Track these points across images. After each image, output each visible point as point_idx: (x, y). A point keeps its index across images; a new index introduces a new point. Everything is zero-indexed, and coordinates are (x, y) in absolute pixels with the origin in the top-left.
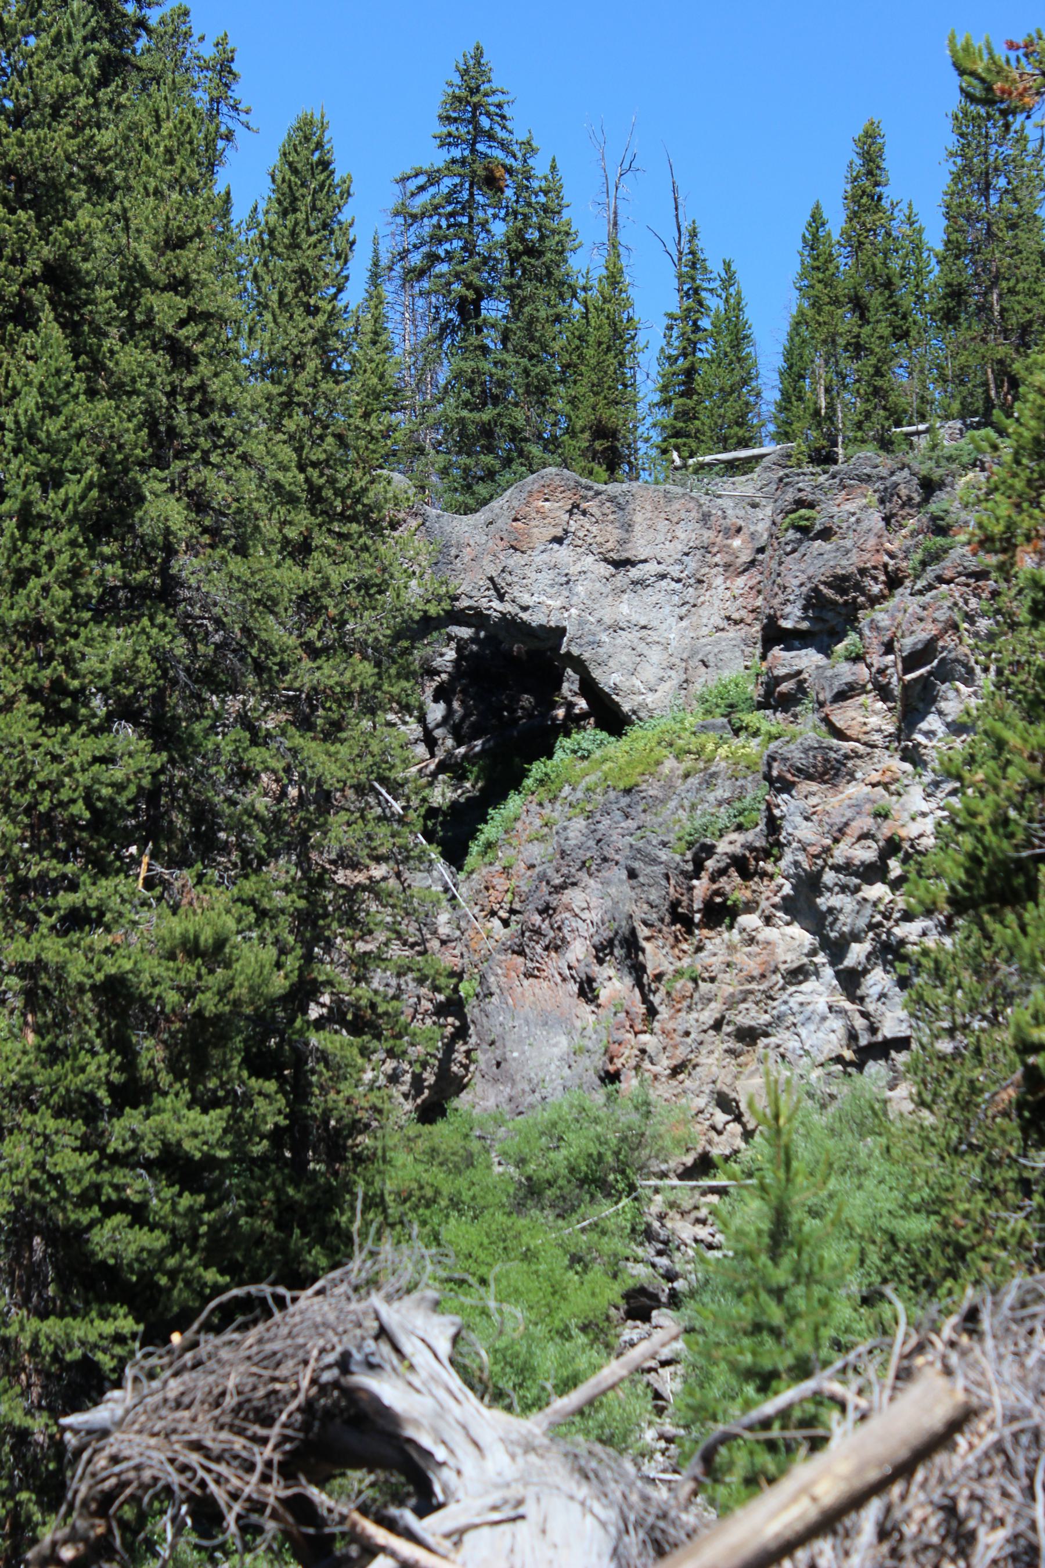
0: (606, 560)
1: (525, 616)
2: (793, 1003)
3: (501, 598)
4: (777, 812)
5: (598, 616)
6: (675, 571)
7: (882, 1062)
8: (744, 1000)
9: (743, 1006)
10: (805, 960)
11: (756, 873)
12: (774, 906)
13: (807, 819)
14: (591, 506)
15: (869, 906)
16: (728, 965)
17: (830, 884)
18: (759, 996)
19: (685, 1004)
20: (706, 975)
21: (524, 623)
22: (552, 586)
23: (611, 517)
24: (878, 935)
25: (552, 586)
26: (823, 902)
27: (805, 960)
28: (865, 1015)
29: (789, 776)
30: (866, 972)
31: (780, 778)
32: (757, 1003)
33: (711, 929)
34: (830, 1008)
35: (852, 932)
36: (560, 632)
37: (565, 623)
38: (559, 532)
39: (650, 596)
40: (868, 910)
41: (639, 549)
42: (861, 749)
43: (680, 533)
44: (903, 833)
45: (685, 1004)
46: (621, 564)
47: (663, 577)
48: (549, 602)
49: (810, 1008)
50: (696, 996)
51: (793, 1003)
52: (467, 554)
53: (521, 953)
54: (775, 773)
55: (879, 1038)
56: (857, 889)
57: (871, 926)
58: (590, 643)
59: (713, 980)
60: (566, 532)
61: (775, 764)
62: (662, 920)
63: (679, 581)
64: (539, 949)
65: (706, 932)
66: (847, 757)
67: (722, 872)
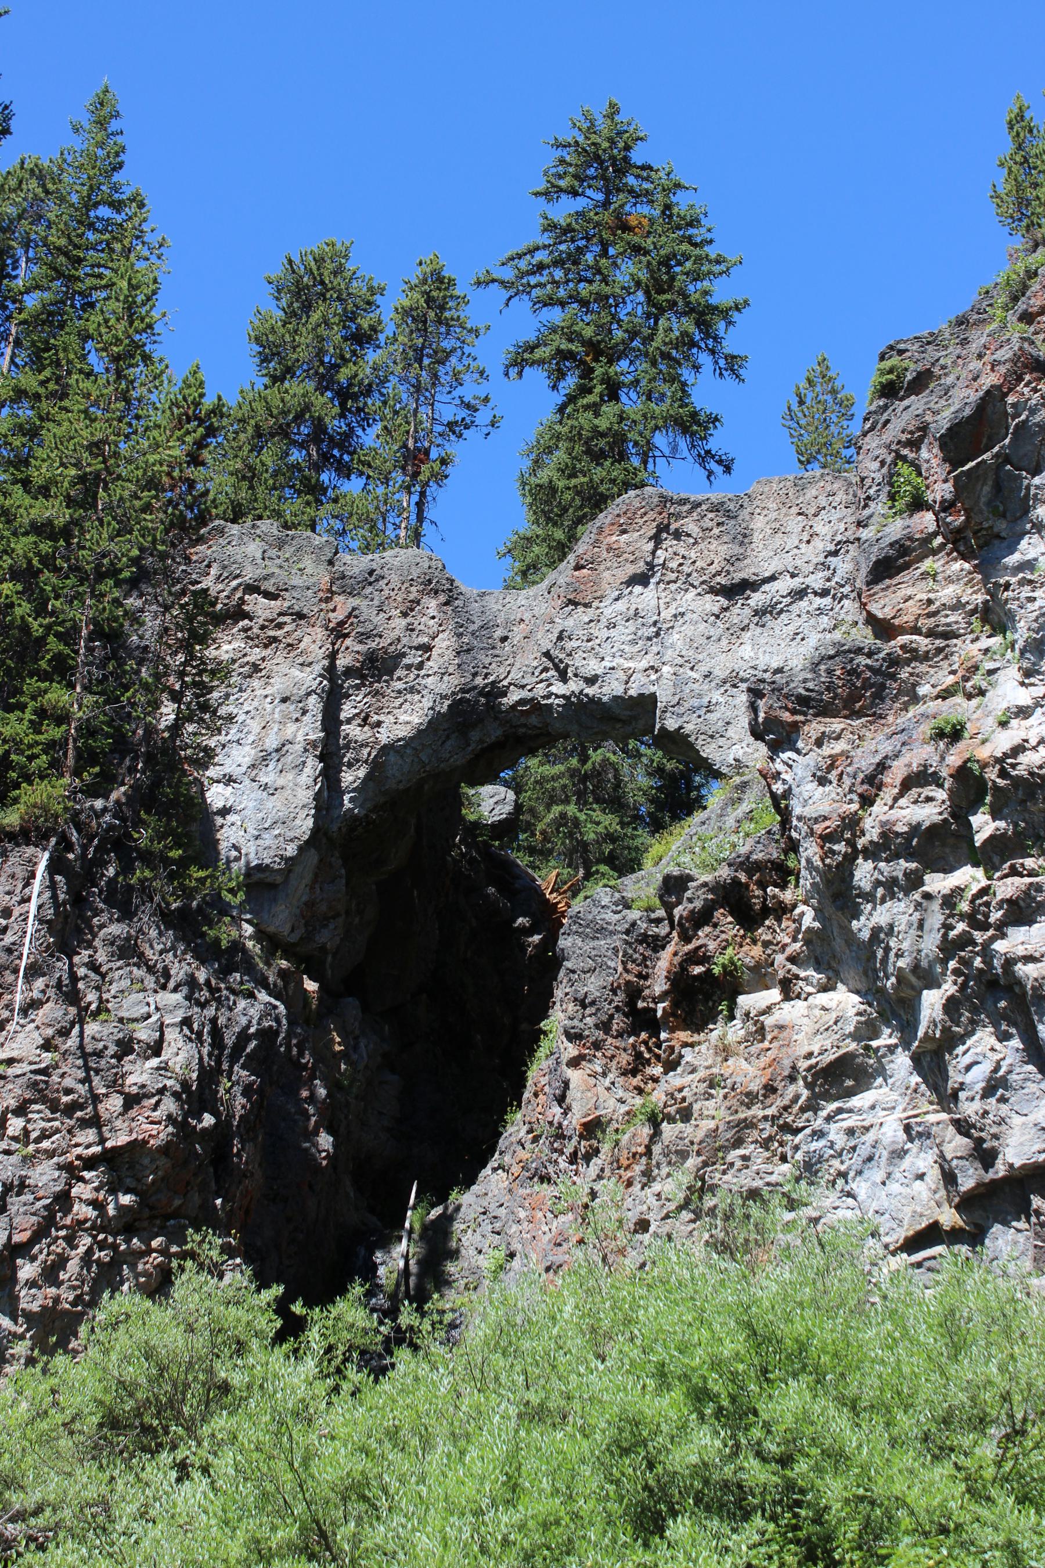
0: (713, 591)
1: (590, 691)
2: (835, 1133)
3: (563, 678)
4: (778, 788)
5: (703, 669)
6: (817, 581)
7: (1022, 1225)
8: (738, 1143)
9: (734, 1155)
10: (852, 1046)
12: (792, 959)
13: (822, 781)
14: (690, 525)
15: (936, 905)
16: (712, 1083)
17: (866, 885)
18: (768, 1130)
19: (638, 1169)
20: (672, 1110)
21: (592, 700)
24: (966, 963)
26: (862, 927)
27: (852, 1046)
28: (963, 1127)
29: (786, 716)
30: (949, 1041)
31: (772, 723)
32: (766, 1144)
33: (699, 1028)
34: (907, 1129)
35: (916, 968)
36: (647, 703)
37: (652, 689)
38: (640, 567)
39: (781, 627)
40: (936, 917)
41: (761, 561)
42: (923, 643)
43: (819, 528)
44: (984, 753)
45: (638, 1169)
46: (736, 591)
47: (800, 594)
48: (631, 664)
49: (870, 1137)
50: (657, 1149)
51: (835, 1133)
52: (517, 633)
53: (545, 1179)
54: (762, 715)
55: (1000, 1170)
56: (914, 881)
57: (950, 948)
58: (693, 710)
59: (686, 1115)
60: (651, 566)
61: (761, 703)
62: (605, 1026)
63: (824, 593)
64: (563, 1164)
65: (683, 1035)
66: (894, 661)
67: (702, 918)
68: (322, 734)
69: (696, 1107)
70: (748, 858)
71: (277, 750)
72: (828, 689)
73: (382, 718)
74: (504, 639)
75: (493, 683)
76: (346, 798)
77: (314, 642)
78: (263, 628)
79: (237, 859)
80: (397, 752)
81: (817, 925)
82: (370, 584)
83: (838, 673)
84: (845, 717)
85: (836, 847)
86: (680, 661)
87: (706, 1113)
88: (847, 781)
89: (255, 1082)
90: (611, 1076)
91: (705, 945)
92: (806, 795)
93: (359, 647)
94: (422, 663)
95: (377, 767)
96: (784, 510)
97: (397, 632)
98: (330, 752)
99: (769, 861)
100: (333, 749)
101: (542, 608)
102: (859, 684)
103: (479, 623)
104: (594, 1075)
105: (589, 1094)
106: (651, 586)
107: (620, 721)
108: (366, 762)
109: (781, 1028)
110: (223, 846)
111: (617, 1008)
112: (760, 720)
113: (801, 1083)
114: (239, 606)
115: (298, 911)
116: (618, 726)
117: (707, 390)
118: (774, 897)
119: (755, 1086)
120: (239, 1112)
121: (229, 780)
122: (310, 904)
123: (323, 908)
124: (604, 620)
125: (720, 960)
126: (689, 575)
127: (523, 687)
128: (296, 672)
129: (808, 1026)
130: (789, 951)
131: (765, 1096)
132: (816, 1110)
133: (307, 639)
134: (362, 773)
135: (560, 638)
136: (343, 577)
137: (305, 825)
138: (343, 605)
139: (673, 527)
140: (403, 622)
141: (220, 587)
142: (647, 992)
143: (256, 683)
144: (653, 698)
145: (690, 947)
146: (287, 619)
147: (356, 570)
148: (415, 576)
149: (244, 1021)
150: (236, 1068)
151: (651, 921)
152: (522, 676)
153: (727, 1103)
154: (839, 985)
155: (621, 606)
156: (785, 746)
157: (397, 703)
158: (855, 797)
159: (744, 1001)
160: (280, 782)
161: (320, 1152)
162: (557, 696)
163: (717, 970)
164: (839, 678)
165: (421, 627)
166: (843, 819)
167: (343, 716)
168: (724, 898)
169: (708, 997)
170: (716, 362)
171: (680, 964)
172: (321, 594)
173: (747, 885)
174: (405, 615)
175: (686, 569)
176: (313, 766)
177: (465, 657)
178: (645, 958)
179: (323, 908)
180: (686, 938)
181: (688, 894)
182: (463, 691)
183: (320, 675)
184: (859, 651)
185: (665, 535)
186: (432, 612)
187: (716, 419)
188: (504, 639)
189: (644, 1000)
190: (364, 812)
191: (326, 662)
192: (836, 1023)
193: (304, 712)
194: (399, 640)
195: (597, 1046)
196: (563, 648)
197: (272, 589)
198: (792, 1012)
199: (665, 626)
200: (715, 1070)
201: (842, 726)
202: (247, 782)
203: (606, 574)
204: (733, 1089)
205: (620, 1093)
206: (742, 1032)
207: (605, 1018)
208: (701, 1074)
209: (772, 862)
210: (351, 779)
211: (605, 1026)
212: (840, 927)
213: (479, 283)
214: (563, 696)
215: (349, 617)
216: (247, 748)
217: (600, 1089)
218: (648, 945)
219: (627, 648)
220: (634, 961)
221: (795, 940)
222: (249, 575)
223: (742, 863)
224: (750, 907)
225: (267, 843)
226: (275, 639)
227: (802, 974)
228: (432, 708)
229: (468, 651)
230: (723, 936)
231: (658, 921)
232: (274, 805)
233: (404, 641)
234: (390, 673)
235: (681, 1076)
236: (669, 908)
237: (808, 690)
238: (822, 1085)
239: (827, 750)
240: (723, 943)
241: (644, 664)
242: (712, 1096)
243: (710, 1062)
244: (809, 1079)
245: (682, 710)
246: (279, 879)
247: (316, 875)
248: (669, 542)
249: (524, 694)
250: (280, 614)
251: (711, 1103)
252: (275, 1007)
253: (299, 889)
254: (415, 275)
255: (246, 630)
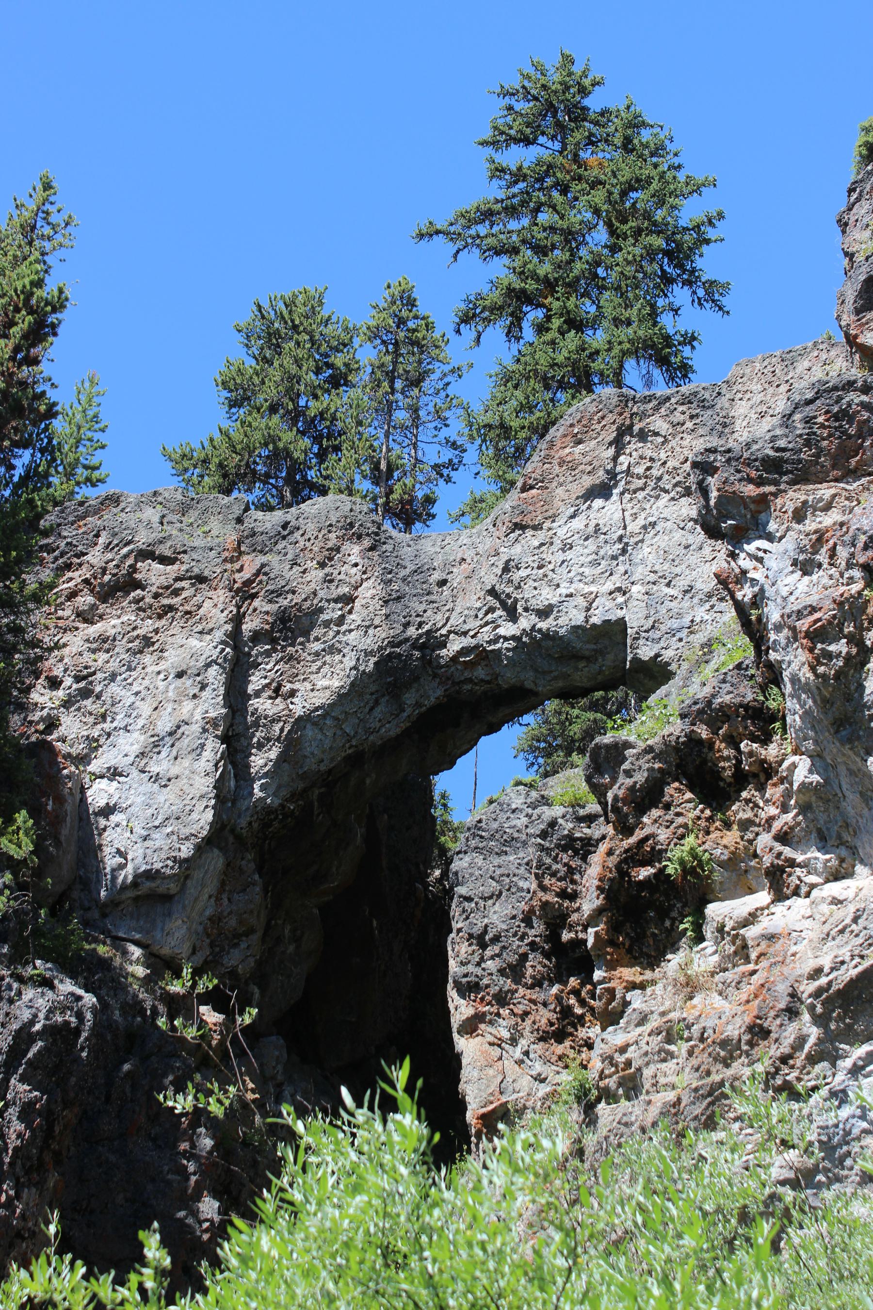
1: (543, 625)
3: (513, 616)
5: (682, 583)
11: (741, 779)
12: (783, 838)
14: (659, 424)
20: (611, 1083)
21: (546, 635)
22: (595, 563)
23: (689, 425)
25: (595, 563)
29: (750, 490)
31: (730, 501)
36: (615, 630)
37: (620, 614)
48: (593, 588)
52: (457, 576)
54: (714, 494)
58: (672, 633)
59: (632, 1086)
61: (713, 482)
62: (515, 971)
65: (629, 973)
67: (648, 797)
68: (224, 711)
69: (647, 1073)
70: (709, 703)
71: (171, 734)
72: (808, 443)
73: (296, 686)
74: (443, 583)
75: (429, 632)
76: (257, 786)
77: (216, 607)
78: (156, 596)
79: (122, 867)
80: (315, 724)
81: (816, 778)
82: (284, 538)
83: (820, 419)
84: (836, 480)
85: (832, 648)
86: (652, 577)
87: (662, 1080)
88: (843, 553)
89: (37, 1100)
90: (523, 1043)
91: (653, 836)
92: (784, 592)
93: (267, 607)
94: (343, 617)
95: (292, 746)
96: (771, 390)
97: (313, 585)
98: (235, 733)
99: (741, 705)
100: (240, 729)
101: (487, 544)
102: (852, 431)
103: (411, 567)
104: (498, 1043)
105: (491, 1072)
106: (615, 497)
107: (582, 658)
108: (278, 739)
109: (771, 938)
110: (107, 850)
111: (533, 946)
112: (712, 502)
113: (806, 1017)
114: (130, 574)
115: (200, 929)
116: (581, 665)
117: (683, 312)
118: (751, 754)
119: (734, 1030)
120: (13, 1141)
121: (114, 773)
122: (216, 920)
123: (233, 922)
124: (558, 543)
125: (678, 852)
126: (659, 479)
127: (465, 634)
128: (194, 643)
129: (812, 931)
130: (777, 825)
131: (751, 1044)
132: (834, 1058)
133: (208, 604)
134: (273, 754)
135: (506, 569)
136: (253, 534)
137: (203, 819)
138: (250, 564)
139: (636, 428)
140: (321, 574)
141: (110, 556)
142: (575, 917)
143: (147, 659)
144: (621, 624)
145: (632, 840)
146: (185, 584)
147: (268, 525)
148: (333, 520)
149: (26, 1015)
150: (13, 1081)
151: (580, 819)
152: (464, 621)
153: (694, 1062)
154: (859, 868)
155: (578, 523)
156: (751, 534)
157: (314, 668)
158: (857, 573)
159: (715, 910)
160: (174, 771)
161: (200, 1222)
162: (506, 639)
163: (671, 869)
164: (822, 426)
165: (342, 577)
166: (841, 604)
167: (251, 688)
168: (678, 766)
169: (663, 913)
170: (694, 293)
171: (618, 867)
172: (226, 554)
173: (711, 744)
174: (322, 565)
175: (655, 472)
176: (213, 748)
177: (393, 606)
178: (571, 871)
179: (233, 922)
180: (626, 830)
181: (626, 766)
182: (392, 644)
183: (222, 642)
184: (850, 385)
185: (628, 438)
186: (353, 559)
187: (694, 338)
188: (443, 583)
189: (571, 928)
190: (277, 802)
191: (229, 627)
192: (855, 920)
193: (203, 687)
194: (315, 593)
195: (502, 999)
196: (510, 581)
197: (168, 553)
198: (789, 915)
199: (632, 541)
200: (674, 1016)
201: (833, 491)
202: (135, 773)
203: (560, 491)
204: (702, 1039)
205: (538, 1067)
206: (716, 958)
207: (513, 959)
208: (655, 1022)
209: (746, 707)
210: (261, 762)
211: (515, 971)
212: (851, 773)
213: (421, 236)
214: (513, 638)
215: (258, 573)
216: (136, 735)
217: (509, 1064)
218: (576, 852)
219: (587, 571)
220: (553, 874)
221: (785, 809)
222: (143, 539)
223: (701, 712)
224: (716, 774)
225: (158, 844)
226: (171, 608)
227: (800, 858)
228: (355, 668)
229: (398, 598)
230: (680, 820)
231: (590, 819)
232: (167, 799)
233: (321, 594)
234: (306, 633)
235: (625, 1030)
236: (599, 791)
237: (778, 450)
238: (840, 1019)
239: (810, 525)
240: (680, 831)
241: (609, 586)
242: (671, 1055)
243: (668, 1004)
244: (819, 1009)
245: (655, 634)
246: (173, 888)
247: (223, 884)
248: (633, 445)
249: (467, 641)
250: (178, 579)
251: (671, 1065)
252: (79, 998)
253: (201, 900)
254: (382, 298)
255: (137, 601)
